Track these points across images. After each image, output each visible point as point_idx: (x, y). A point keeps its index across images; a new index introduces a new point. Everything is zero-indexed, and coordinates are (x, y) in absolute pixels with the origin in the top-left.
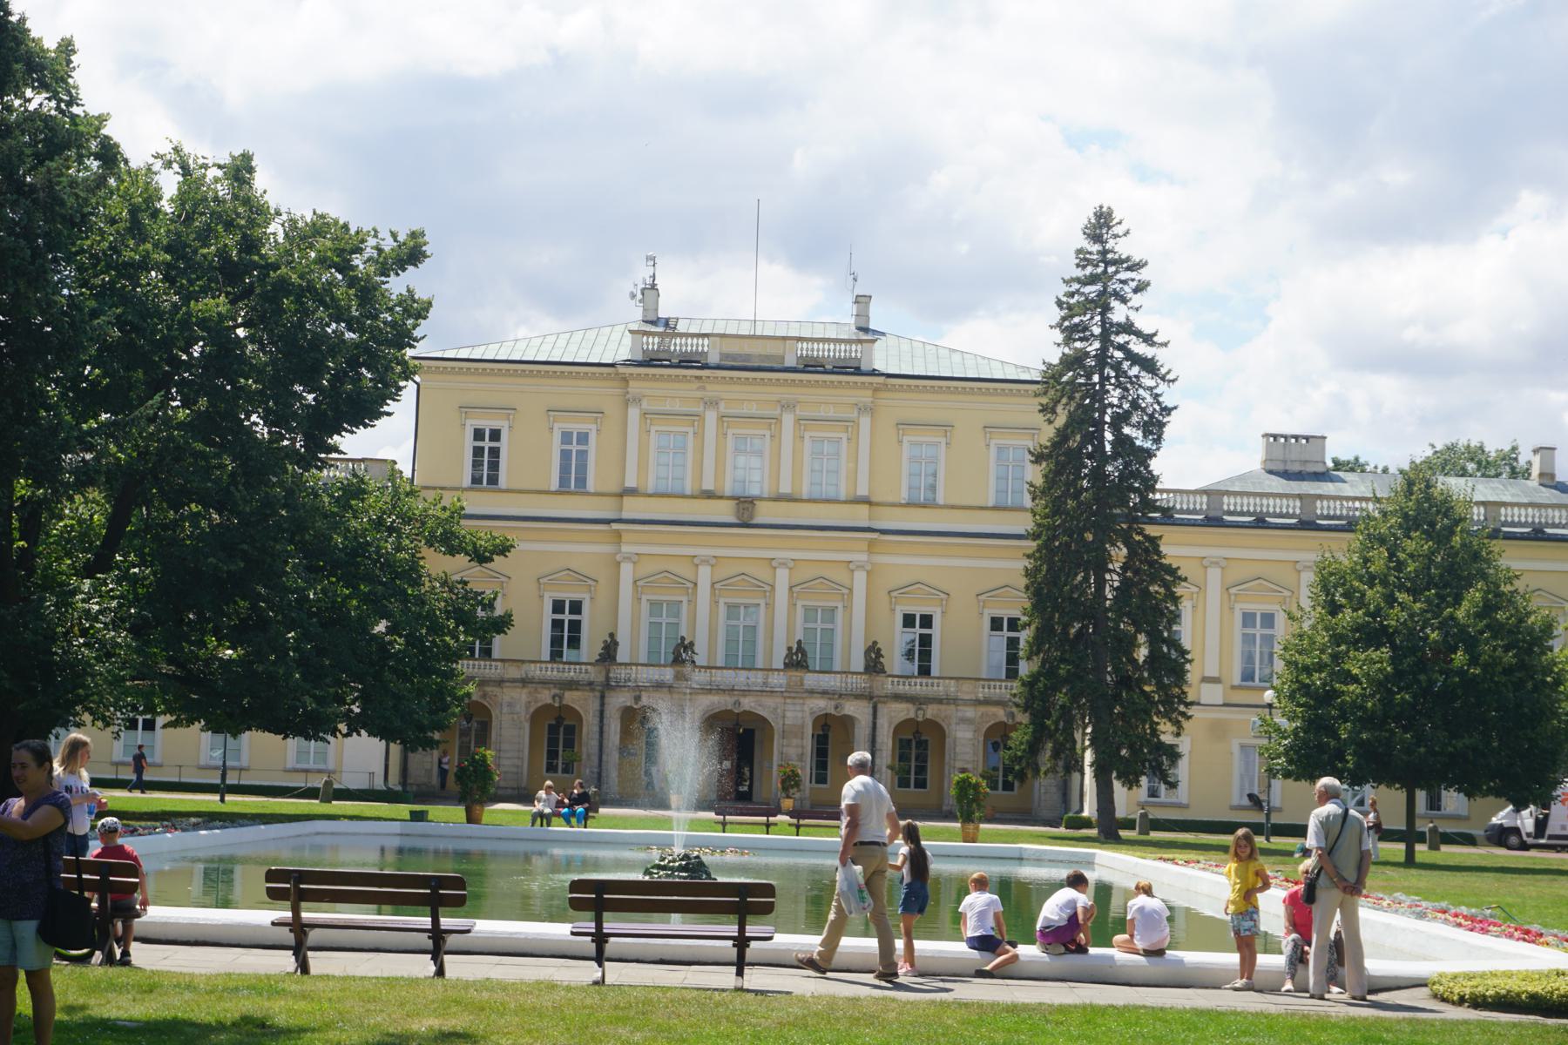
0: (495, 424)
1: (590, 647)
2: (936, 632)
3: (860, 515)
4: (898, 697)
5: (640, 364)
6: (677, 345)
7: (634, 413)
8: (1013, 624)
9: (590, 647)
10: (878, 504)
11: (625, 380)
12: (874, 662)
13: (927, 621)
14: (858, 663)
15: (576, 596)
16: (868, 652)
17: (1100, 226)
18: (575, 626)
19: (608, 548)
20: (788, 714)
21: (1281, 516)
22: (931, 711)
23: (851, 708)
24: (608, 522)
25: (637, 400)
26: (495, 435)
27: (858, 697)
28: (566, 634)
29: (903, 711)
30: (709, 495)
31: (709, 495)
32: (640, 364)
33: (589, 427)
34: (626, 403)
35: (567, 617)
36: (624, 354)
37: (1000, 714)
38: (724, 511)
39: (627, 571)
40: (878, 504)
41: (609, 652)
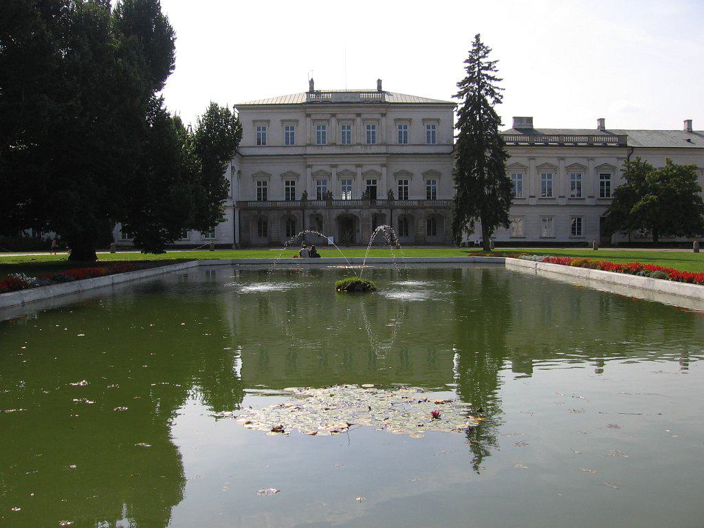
1: (299, 197)
2: (408, 186)
3: (383, 150)
4: (398, 208)
6: (321, 98)
9: (299, 197)
10: (388, 145)
12: (390, 194)
13: (608, 176)
14: (385, 197)
16: (388, 194)
17: (477, 37)
18: (293, 189)
20: (364, 214)
21: (523, 142)
22: (409, 212)
23: (384, 211)
24: (302, 155)
27: (386, 208)
28: (290, 193)
29: (400, 212)
31: (334, 144)
35: (290, 186)
36: (304, 100)
37: (432, 211)
40: (388, 145)
41: (305, 195)
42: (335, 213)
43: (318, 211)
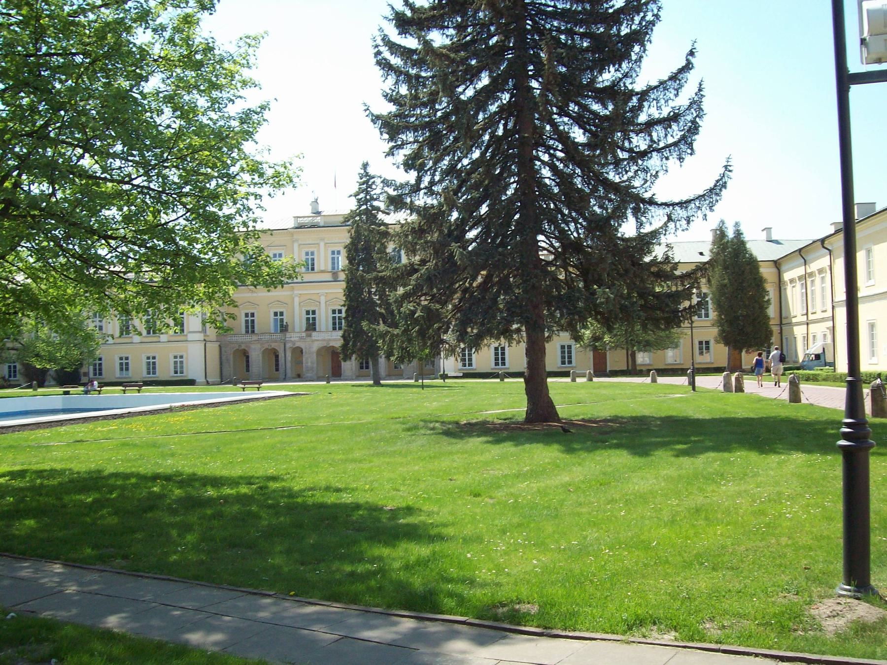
0: (312, 250)
5: (297, 228)
7: (296, 245)
8: (340, 312)
11: (292, 234)
15: (281, 310)
19: (289, 293)
25: (297, 240)
26: (312, 253)
30: (322, 272)
31: (322, 272)
32: (297, 228)
33: (282, 252)
34: (293, 242)
38: (328, 277)
39: (297, 300)
42: (315, 347)
43: (297, 345)
